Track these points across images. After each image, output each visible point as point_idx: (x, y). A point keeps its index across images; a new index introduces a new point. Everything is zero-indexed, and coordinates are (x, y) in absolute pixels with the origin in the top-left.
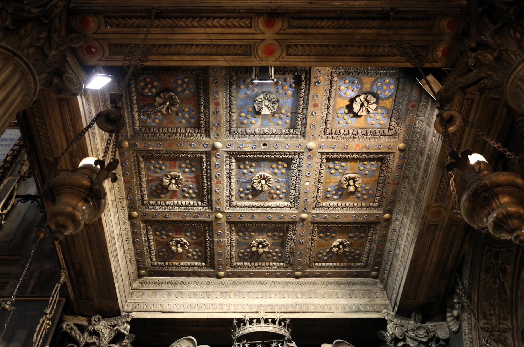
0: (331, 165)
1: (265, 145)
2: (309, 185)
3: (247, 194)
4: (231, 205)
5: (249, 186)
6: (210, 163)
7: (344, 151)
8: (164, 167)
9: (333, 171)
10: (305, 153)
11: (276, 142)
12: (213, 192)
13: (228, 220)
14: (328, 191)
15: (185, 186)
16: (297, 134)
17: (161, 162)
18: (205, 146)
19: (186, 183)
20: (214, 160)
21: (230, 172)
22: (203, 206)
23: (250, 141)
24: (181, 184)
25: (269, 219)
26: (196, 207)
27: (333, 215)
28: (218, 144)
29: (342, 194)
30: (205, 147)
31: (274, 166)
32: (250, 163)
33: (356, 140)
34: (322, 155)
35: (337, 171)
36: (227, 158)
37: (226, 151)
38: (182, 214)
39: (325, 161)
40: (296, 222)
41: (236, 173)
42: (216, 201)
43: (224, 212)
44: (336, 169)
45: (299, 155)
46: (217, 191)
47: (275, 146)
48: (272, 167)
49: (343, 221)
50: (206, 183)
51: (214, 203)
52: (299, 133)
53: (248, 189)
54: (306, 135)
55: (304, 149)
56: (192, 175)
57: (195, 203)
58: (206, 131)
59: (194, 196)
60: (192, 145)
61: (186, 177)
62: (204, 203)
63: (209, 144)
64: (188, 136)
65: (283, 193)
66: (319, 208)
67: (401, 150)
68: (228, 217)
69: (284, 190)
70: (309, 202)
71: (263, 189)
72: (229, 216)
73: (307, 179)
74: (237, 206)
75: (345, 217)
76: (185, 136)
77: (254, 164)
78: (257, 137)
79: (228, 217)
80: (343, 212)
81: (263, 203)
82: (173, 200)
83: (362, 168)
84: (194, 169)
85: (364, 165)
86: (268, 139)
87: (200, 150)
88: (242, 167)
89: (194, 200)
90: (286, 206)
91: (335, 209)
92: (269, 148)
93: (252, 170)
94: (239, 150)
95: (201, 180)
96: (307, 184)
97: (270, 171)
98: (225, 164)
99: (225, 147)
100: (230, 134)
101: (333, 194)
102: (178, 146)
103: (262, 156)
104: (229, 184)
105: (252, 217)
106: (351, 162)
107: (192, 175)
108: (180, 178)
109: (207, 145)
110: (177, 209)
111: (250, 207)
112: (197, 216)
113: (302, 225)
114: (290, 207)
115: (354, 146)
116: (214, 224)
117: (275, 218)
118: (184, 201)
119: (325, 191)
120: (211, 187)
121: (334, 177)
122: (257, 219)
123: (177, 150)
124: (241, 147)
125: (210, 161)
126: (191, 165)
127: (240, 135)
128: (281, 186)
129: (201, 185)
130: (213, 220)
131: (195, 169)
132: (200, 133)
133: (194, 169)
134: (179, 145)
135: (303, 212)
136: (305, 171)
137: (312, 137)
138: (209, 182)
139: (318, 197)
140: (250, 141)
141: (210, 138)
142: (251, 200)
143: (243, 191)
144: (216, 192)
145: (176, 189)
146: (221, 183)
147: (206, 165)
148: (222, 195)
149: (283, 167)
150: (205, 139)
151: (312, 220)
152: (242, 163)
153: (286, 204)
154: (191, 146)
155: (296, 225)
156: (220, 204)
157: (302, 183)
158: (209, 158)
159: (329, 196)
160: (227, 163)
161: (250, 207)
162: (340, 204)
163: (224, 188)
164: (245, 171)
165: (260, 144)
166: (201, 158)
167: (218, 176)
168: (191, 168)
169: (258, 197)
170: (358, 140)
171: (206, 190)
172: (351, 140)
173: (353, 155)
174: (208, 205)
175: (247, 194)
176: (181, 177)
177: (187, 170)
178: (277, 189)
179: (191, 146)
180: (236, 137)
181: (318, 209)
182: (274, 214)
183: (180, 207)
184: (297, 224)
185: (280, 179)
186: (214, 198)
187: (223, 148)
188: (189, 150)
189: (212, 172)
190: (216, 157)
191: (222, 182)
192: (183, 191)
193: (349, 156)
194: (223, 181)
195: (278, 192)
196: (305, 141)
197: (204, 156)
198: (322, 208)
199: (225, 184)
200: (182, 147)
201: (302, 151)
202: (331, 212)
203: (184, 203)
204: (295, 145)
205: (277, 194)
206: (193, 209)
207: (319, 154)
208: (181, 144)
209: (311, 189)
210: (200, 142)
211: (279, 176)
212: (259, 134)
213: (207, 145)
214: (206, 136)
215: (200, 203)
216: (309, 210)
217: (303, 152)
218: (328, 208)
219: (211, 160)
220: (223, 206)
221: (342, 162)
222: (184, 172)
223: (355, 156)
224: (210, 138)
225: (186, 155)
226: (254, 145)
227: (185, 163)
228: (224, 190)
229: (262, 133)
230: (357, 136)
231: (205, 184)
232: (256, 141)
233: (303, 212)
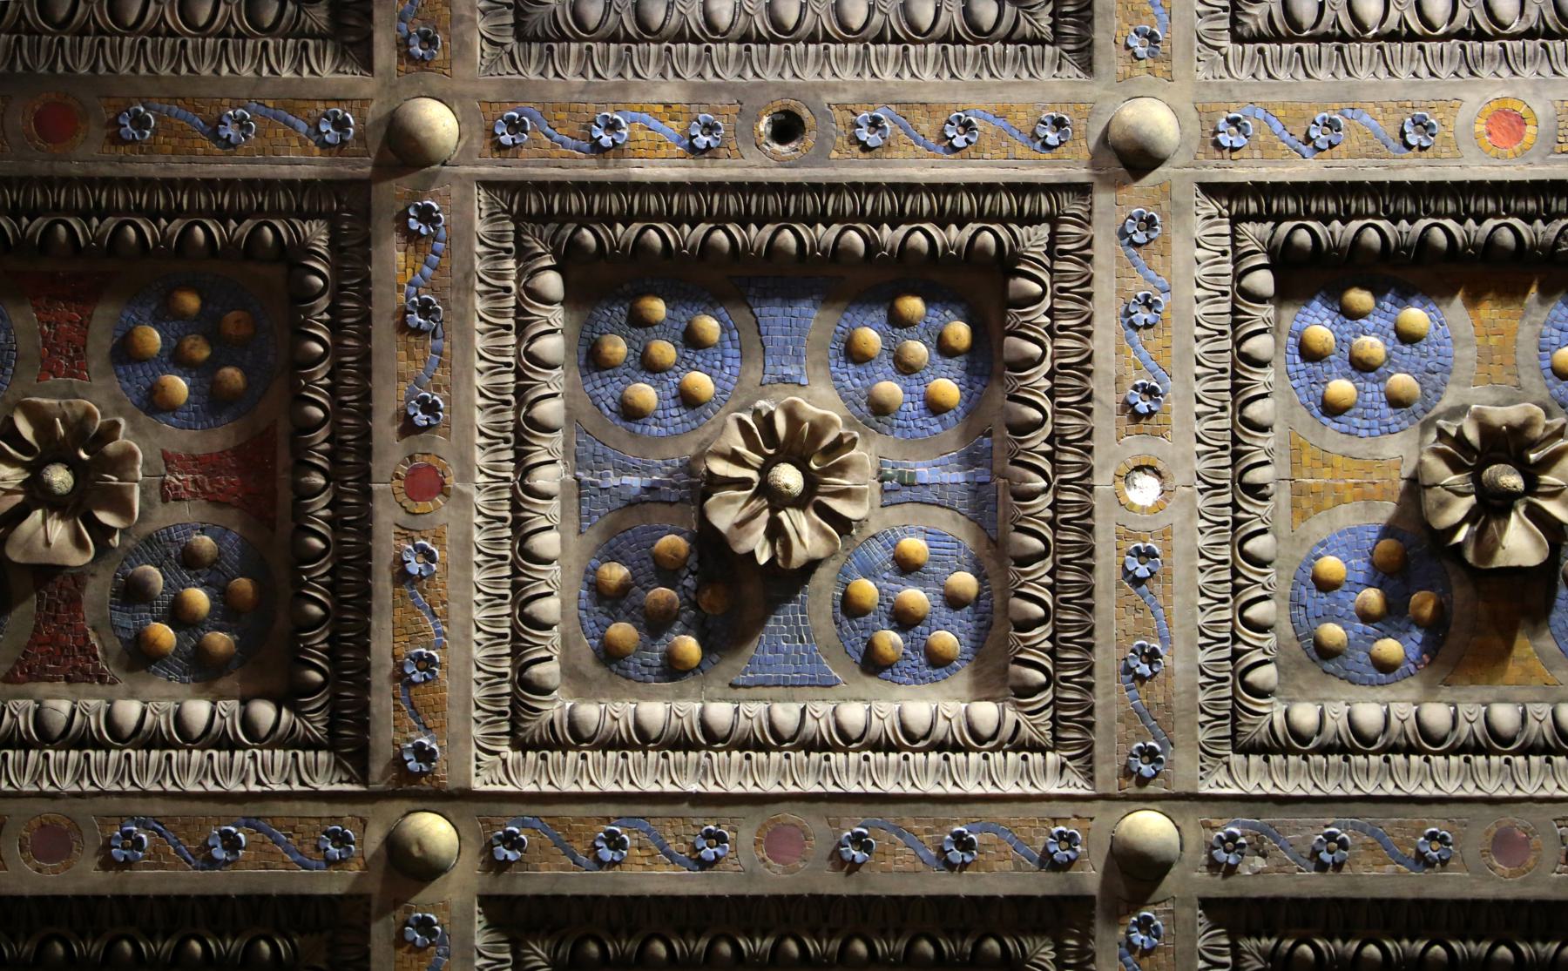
0: (1321, 328)
1: (787, 128)
2: (1158, 507)
3: (656, 624)
4: (533, 727)
5: (672, 542)
6: (366, 298)
7: (1408, 176)
9: (1341, 388)
11: (871, 102)
12: (383, 583)
13: (500, 887)
14: (1325, 585)
15: (152, 546)
16: (1025, 28)
18: (332, 136)
19: (165, 517)
21: (520, 392)
22: (291, 741)
23: (670, 91)
24: (123, 508)
25: (854, 866)
26: (232, 745)
27: (1388, 822)
29: (1439, 608)
30: (324, 145)
31: (870, 337)
32: (682, 316)
33: (1485, 72)
34: (1236, 220)
35: (1374, 392)
36: (496, 255)
37: (487, 184)
38: (105, 819)
39: (1263, 281)
40: (1080, 905)
41: (571, 415)
42: (400, 676)
43: (468, 795)
45: (1053, 220)
46: (414, 567)
47: (864, 134)
49: (1487, 891)
50: (322, 500)
51: (382, 701)
52: (1044, 22)
53: (666, 571)
54: (1099, 37)
55: (1094, 163)
56: (217, 439)
57: (230, 707)
59: (220, 640)
60: (230, 131)
61: (167, 457)
62: (297, 711)
63: (361, 118)
64: (199, 53)
65: (954, 601)
66: (1264, 750)
68: (502, 852)
69: (965, 581)
70: (1179, 685)
71: (787, 547)
72: (512, 841)
73: (1137, 447)
74: (576, 737)
75: (1504, 843)
76: (179, 55)
78: (725, 62)
79: (502, 852)
80: (1470, 790)
81: (795, 708)
82: (43, 688)
84: (232, 376)
86: (809, 75)
87: (285, 171)
89: (223, 684)
90: (987, 728)
91: (1398, 759)
92: (821, 157)
94: (592, 171)
95: (284, 458)
96: (1145, 491)
97: (841, 389)
98: (480, 305)
99: (479, 143)
100: (521, 37)
101: (1365, 617)
102: (116, 139)
103: (769, 229)
104: (516, 507)
105: (708, 853)
106: (1473, 300)
107: (217, 439)
108: (111, 447)
109: (340, 125)
110: (63, 767)
111: (682, 743)
112: (231, 843)
113: (1138, 937)
114: (1019, 744)
115: (1481, 128)
116: (380, 933)
117: (903, 857)
118: (131, 695)
119: (1297, 582)
120: (365, 529)
121: (1359, 447)
122: (750, 876)
123: (105, 170)
124: (606, 140)
125: (367, 281)
126: (214, 337)
127: (598, 47)
129: (286, 527)
130: (374, 887)
131: (246, 373)
132: (298, 32)
134: (128, 130)
135: (1132, 789)
136: (1112, 370)
137: (1141, 51)
138: (351, 485)
139: (1247, 635)
140: (670, 91)
141: (367, 65)
142: (690, 684)
143: (624, 589)
144: (402, 576)
145: (77, 559)
146: (443, 489)
147: (335, 327)
148: (454, 607)
150: (327, 72)
151: (1218, 887)
152: (620, 311)
153: (986, 713)
154: (215, 136)
155: (1085, 937)
156: (438, 707)
157: (1102, 482)
159: (1333, 632)
160: (496, 294)
161: (682, 743)
162: (1437, 715)
163: (467, 543)
165: (748, 116)
167: (421, 419)
168: (213, 365)
169: (750, 650)
170: (1504, 72)
171: (322, 568)
172: (1444, 72)
173: (1480, 220)
174: (332, 726)
175: (656, 624)
176: (124, 439)
178: (906, 567)
179: (215, 136)
180: (565, 57)
181: (1255, 760)
182: (891, 811)
183: (96, 756)
184: (1099, 928)
185: (925, 473)
186: (383, 646)
187: (466, 153)
188: (201, 170)
189: (377, 380)
190: (412, 237)
191: (452, 482)
192: (132, 593)
193: (1450, 223)
194: (466, 477)
195: (915, 596)
196: (1091, 90)
197: (317, 234)
198: (1286, 751)
199: (480, 499)
200: (151, 149)
201: (1080, 174)
202: (1369, 788)
203: (129, 711)
204: (1023, 119)
205: (904, 620)
206: (206, 772)
207: (1212, 208)
208: (140, 122)
209: (1179, 543)
210: (291, 101)
211: (914, 442)
212: (745, 38)
213: (340, 125)
214: (342, 56)
215: (264, 712)
216: (1185, 771)
218: (1345, 750)
219: (374, 269)
220: (455, 726)
221: (1405, 295)
223: (1506, 230)
224: (367, 65)
225: (177, 226)
226: (710, 128)
228: (466, 565)
229: (761, 24)
230: (1492, 47)
231: (320, 507)
232: (716, 89)
233: (1132, 789)
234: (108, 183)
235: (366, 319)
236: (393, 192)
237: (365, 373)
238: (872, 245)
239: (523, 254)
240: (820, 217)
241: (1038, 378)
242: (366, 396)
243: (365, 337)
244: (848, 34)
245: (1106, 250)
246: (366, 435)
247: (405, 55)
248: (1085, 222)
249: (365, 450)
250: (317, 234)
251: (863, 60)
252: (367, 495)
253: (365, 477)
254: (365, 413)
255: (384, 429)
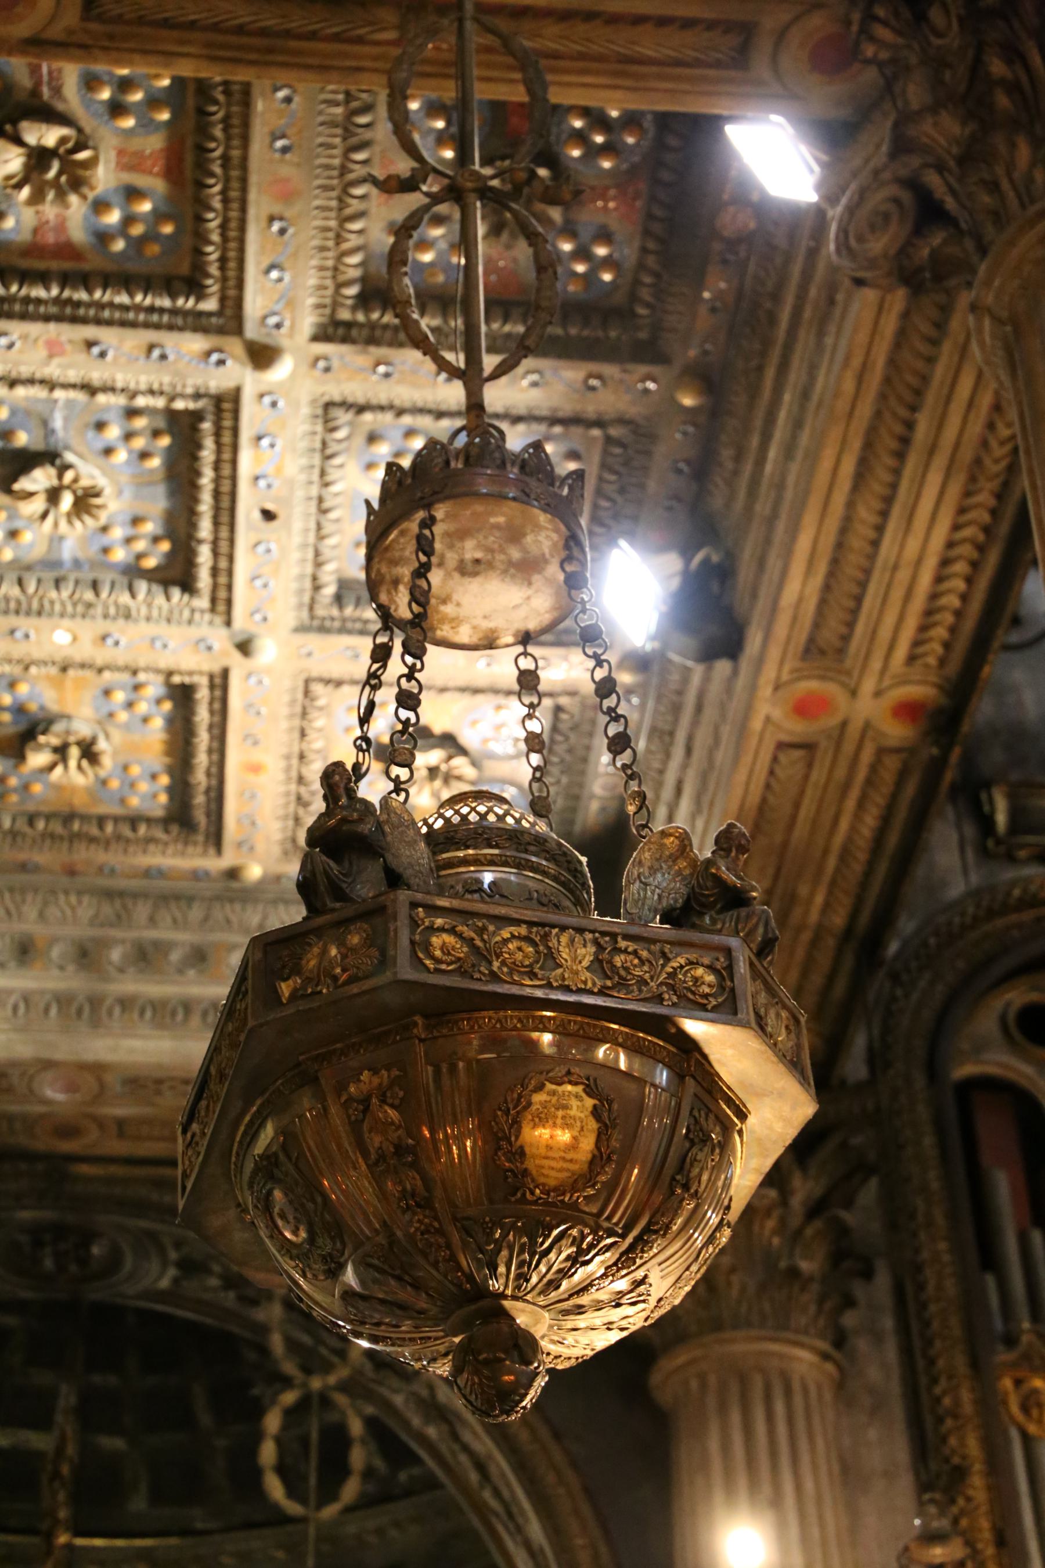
6: (171, 327)
8: (129, 122)
10: (223, 632)
17: (165, 116)
18: (272, 320)
20: (195, 343)
28: (282, 371)
30: (265, 317)
39: (177, 679)
44: (130, 705)
48: (136, 521)
58: (349, 325)
60: (274, 274)
67: (233, 874)
77: (155, 462)
83: (135, 770)
85: (154, 777)
88: (140, 423)
93: (121, 456)
102: (271, 219)
109: (278, 326)
120: (24, 316)
125: (181, 329)
128: (32, 545)
133: (119, 245)
138: (53, 310)
141: (316, 338)
146: (51, 356)
149: (140, 556)
150: (308, 321)
157: (66, 622)
158: (197, 323)
164: (113, 432)
166: (195, 286)
177: (113, 217)
190: (208, 354)
210: (291, 303)
217: (228, 623)
222: (100, 206)
223: (202, 759)
224: (316, 338)
227: (158, 216)
231: (39, 292)
234: (243, 209)
235: (157, 327)
236: (235, 346)
237: (123, 324)
238: (200, 542)
239: (197, 396)
240: (216, 523)
241: (125, 598)
242: (109, 323)
243: (147, 325)
244: (321, 538)
245: (194, 632)
246: (84, 321)
247: (317, 359)
248: (211, 623)
249: (74, 320)
250: (210, 305)
251: (304, 546)
252: (47, 319)
253: (59, 319)
254: (99, 322)
255: (90, 332)
